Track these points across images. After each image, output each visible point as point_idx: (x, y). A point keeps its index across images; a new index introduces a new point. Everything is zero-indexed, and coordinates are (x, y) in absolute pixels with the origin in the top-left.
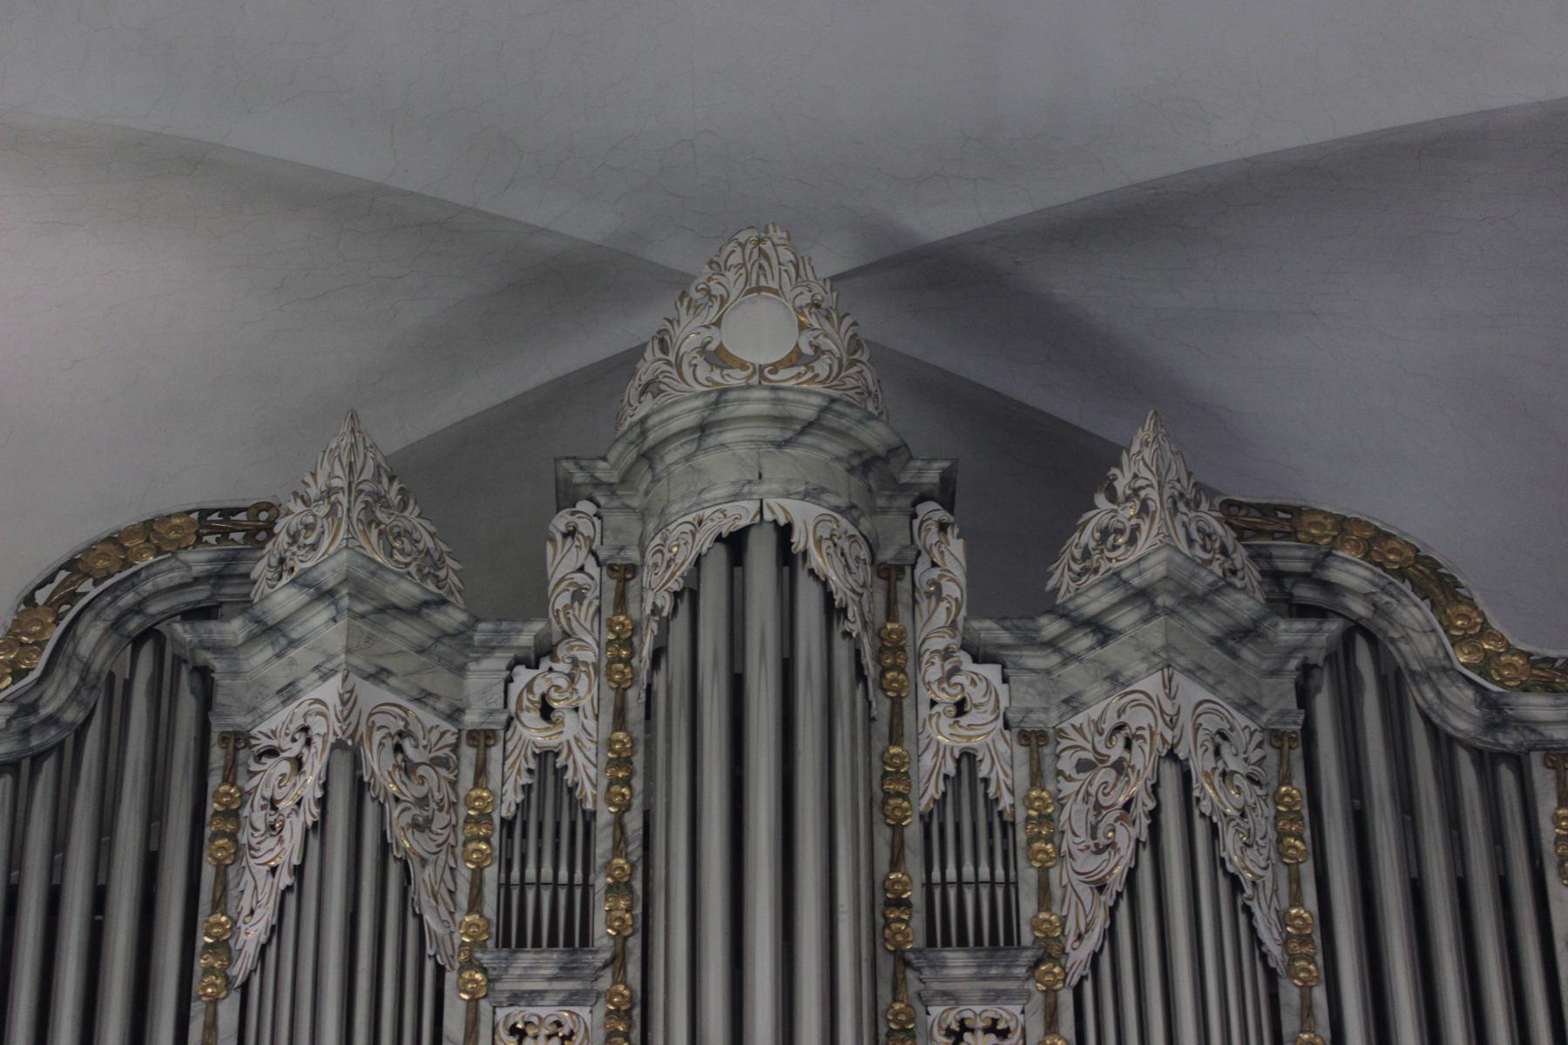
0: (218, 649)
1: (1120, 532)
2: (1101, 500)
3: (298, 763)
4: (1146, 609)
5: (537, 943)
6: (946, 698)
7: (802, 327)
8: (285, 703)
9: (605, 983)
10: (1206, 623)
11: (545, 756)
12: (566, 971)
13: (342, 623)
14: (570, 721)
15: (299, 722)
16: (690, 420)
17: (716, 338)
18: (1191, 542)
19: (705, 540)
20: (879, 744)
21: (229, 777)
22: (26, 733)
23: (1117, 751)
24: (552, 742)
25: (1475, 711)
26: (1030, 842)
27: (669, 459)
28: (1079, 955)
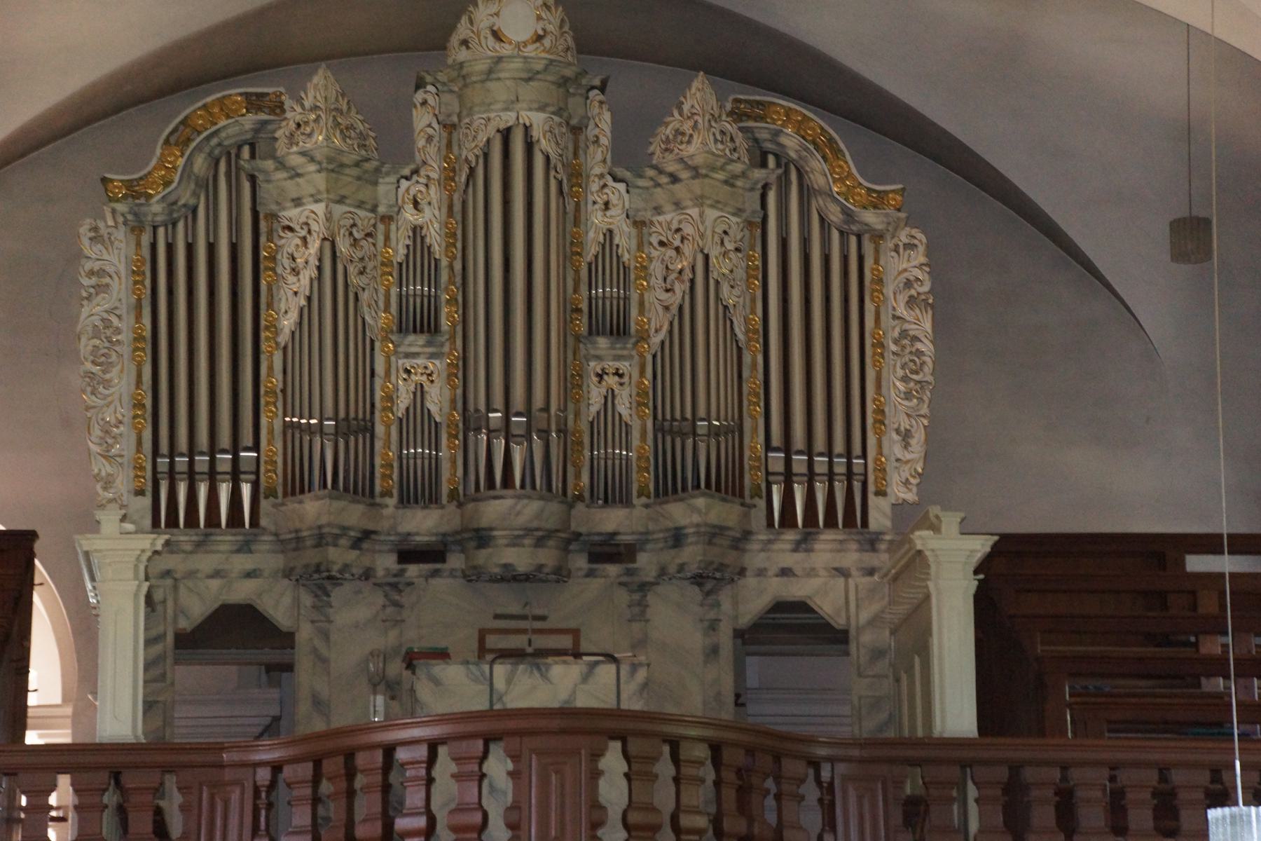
0: (260, 171)
1: (683, 134)
2: (676, 113)
3: (304, 239)
5: (415, 331)
7: (539, 18)
9: (446, 349)
10: (721, 176)
11: (416, 230)
12: (429, 344)
14: (427, 209)
15: (303, 219)
17: (499, 24)
18: (716, 141)
19: (491, 131)
20: (569, 226)
21: (270, 240)
23: (677, 243)
28: (656, 340)
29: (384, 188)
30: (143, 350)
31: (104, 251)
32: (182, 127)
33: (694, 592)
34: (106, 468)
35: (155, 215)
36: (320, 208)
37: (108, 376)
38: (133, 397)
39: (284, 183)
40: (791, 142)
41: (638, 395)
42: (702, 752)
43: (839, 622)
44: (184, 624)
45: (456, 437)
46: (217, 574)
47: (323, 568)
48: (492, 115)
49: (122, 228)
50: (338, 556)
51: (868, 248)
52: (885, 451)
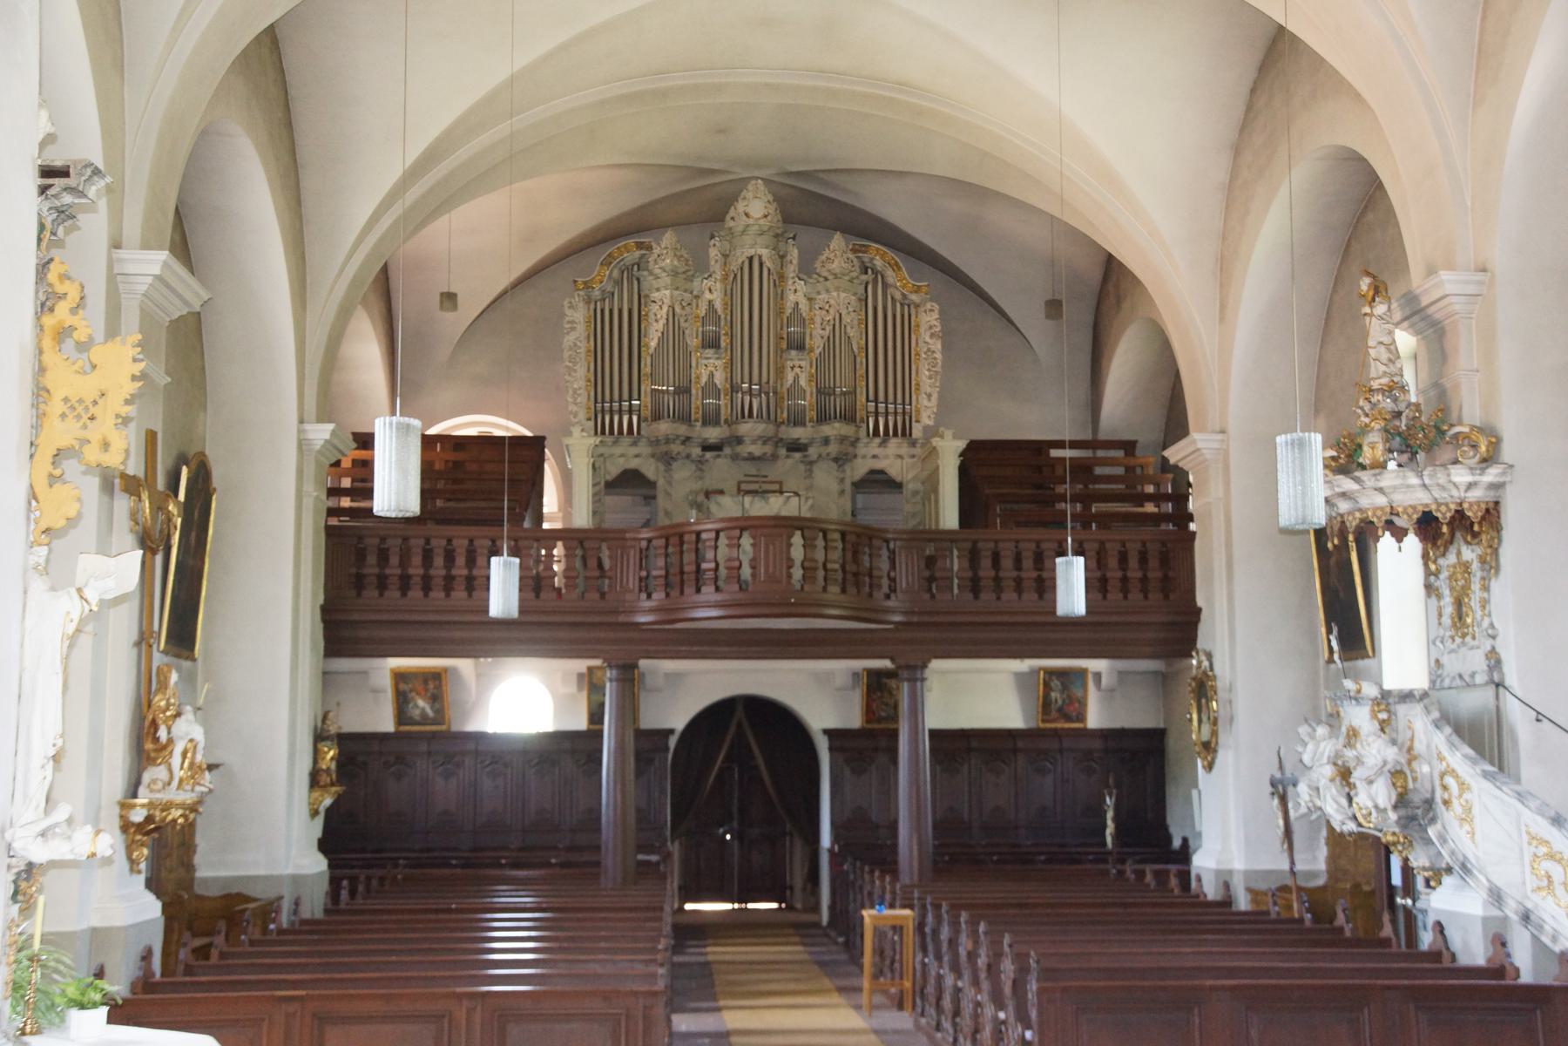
17: (748, 210)
19: (744, 258)
29: (696, 283)
33: (834, 465)
34: (575, 409)
36: (667, 292)
40: (878, 263)
42: (837, 536)
43: (898, 479)
44: (609, 478)
46: (622, 455)
50: (676, 448)
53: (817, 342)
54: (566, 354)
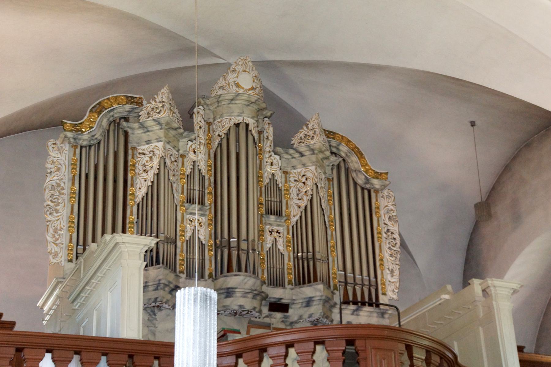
0: (131, 128)
1: (309, 136)
2: (305, 128)
4: (312, 152)
6: (270, 161)
8: (147, 144)
11: (194, 162)
13: (162, 130)
14: (200, 155)
16: (231, 97)
21: (133, 158)
22: (90, 141)
23: (304, 180)
24: (196, 159)
25: (364, 180)
26: (285, 194)
27: (223, 103)
28: (294, 220)
29: (182, 142)
30: (74, 198)
31: (59, 154)
32: (98, 106)
34: (56, 249)
35: (84, 140)
36: (160, 145)
37: (58, 208)
38: (70, 218)
39: (141, 135)
41: (287, 241)
45: (212, 251)
47: (158, 300)
48: (232, 118)
49: (67, 145)
51: (373, 195)
52: (385, 277)
53: (294, 208)
54: (47, 194)
